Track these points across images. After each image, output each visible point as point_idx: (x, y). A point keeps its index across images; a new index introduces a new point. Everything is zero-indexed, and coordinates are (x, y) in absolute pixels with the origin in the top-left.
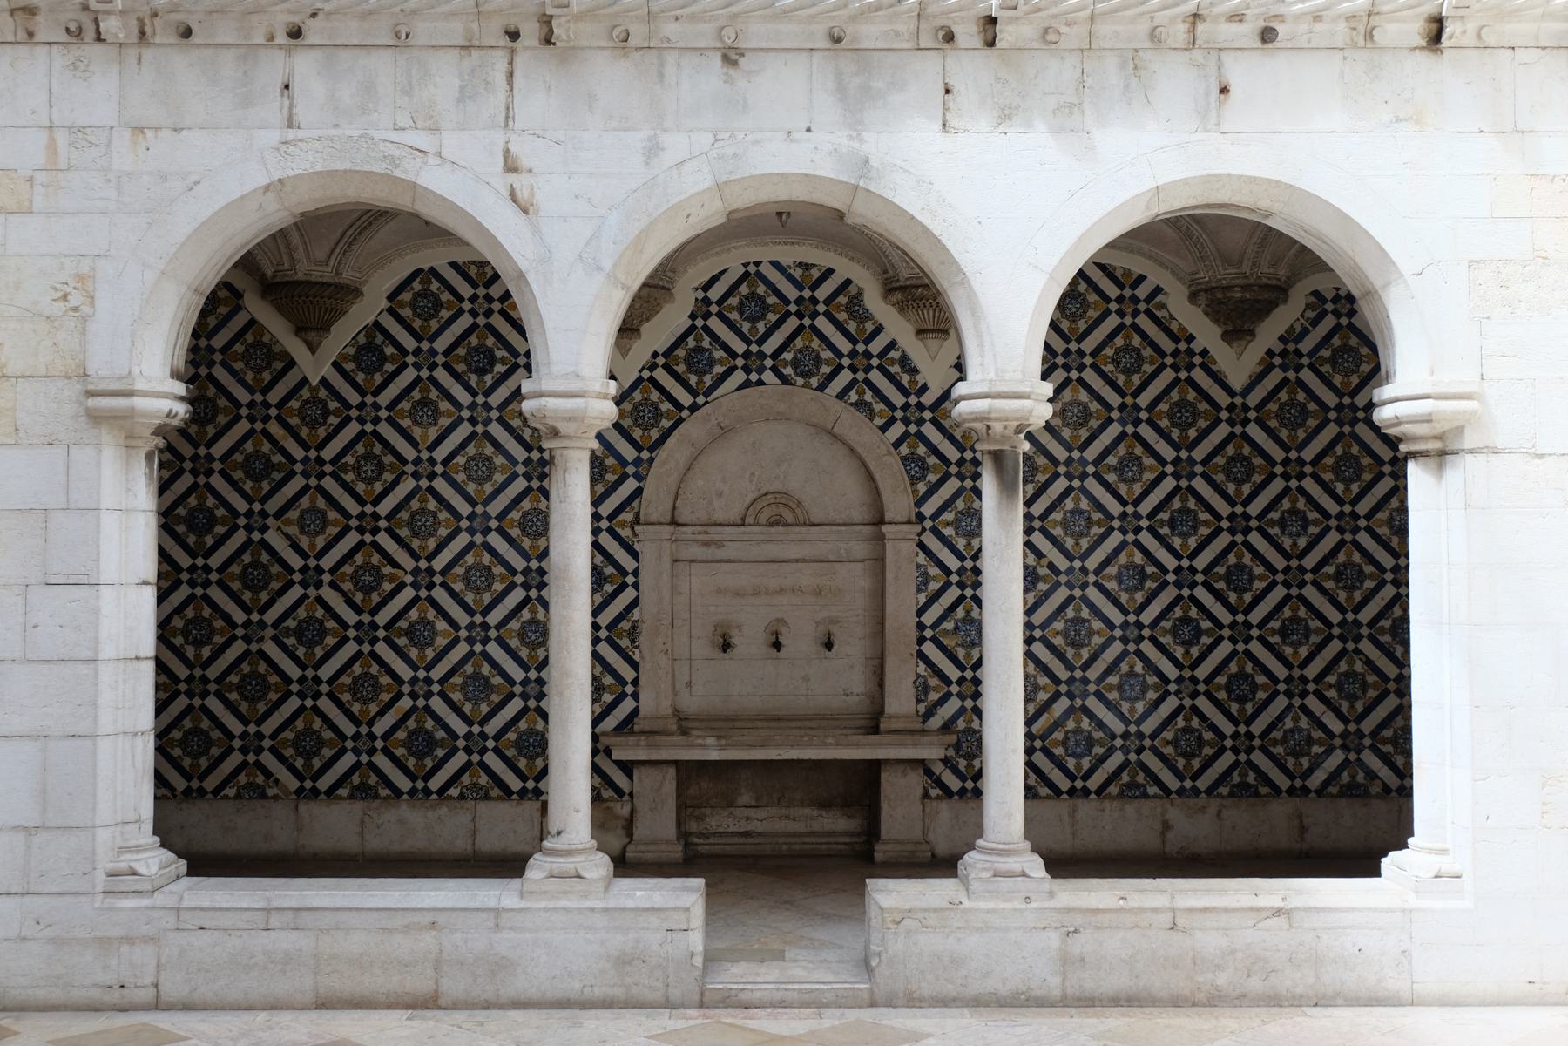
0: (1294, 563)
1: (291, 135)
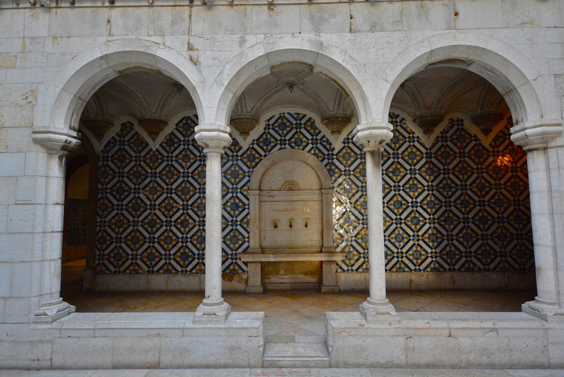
0: (448, 200)
1: (110, 38)
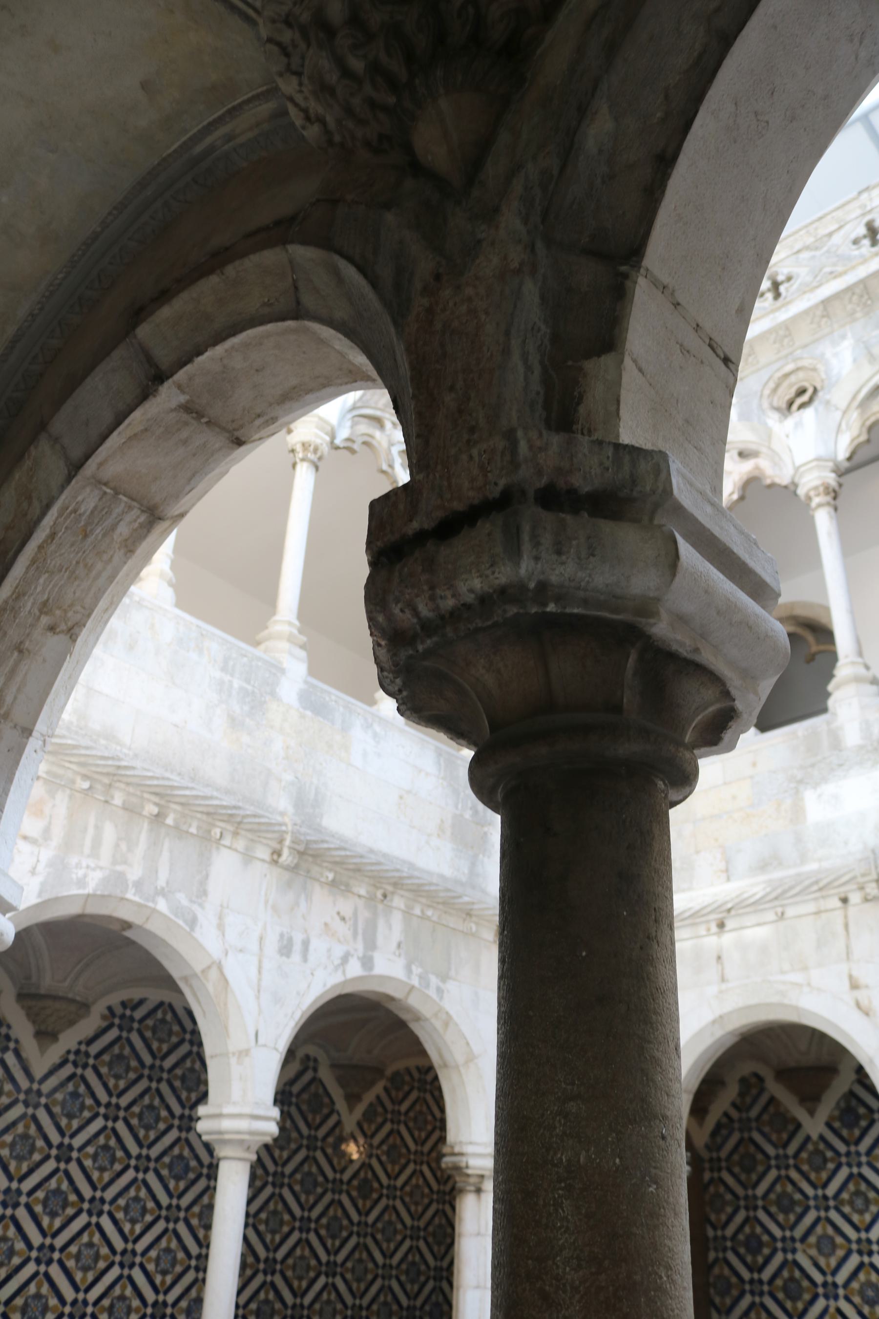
1: (724, 986)
